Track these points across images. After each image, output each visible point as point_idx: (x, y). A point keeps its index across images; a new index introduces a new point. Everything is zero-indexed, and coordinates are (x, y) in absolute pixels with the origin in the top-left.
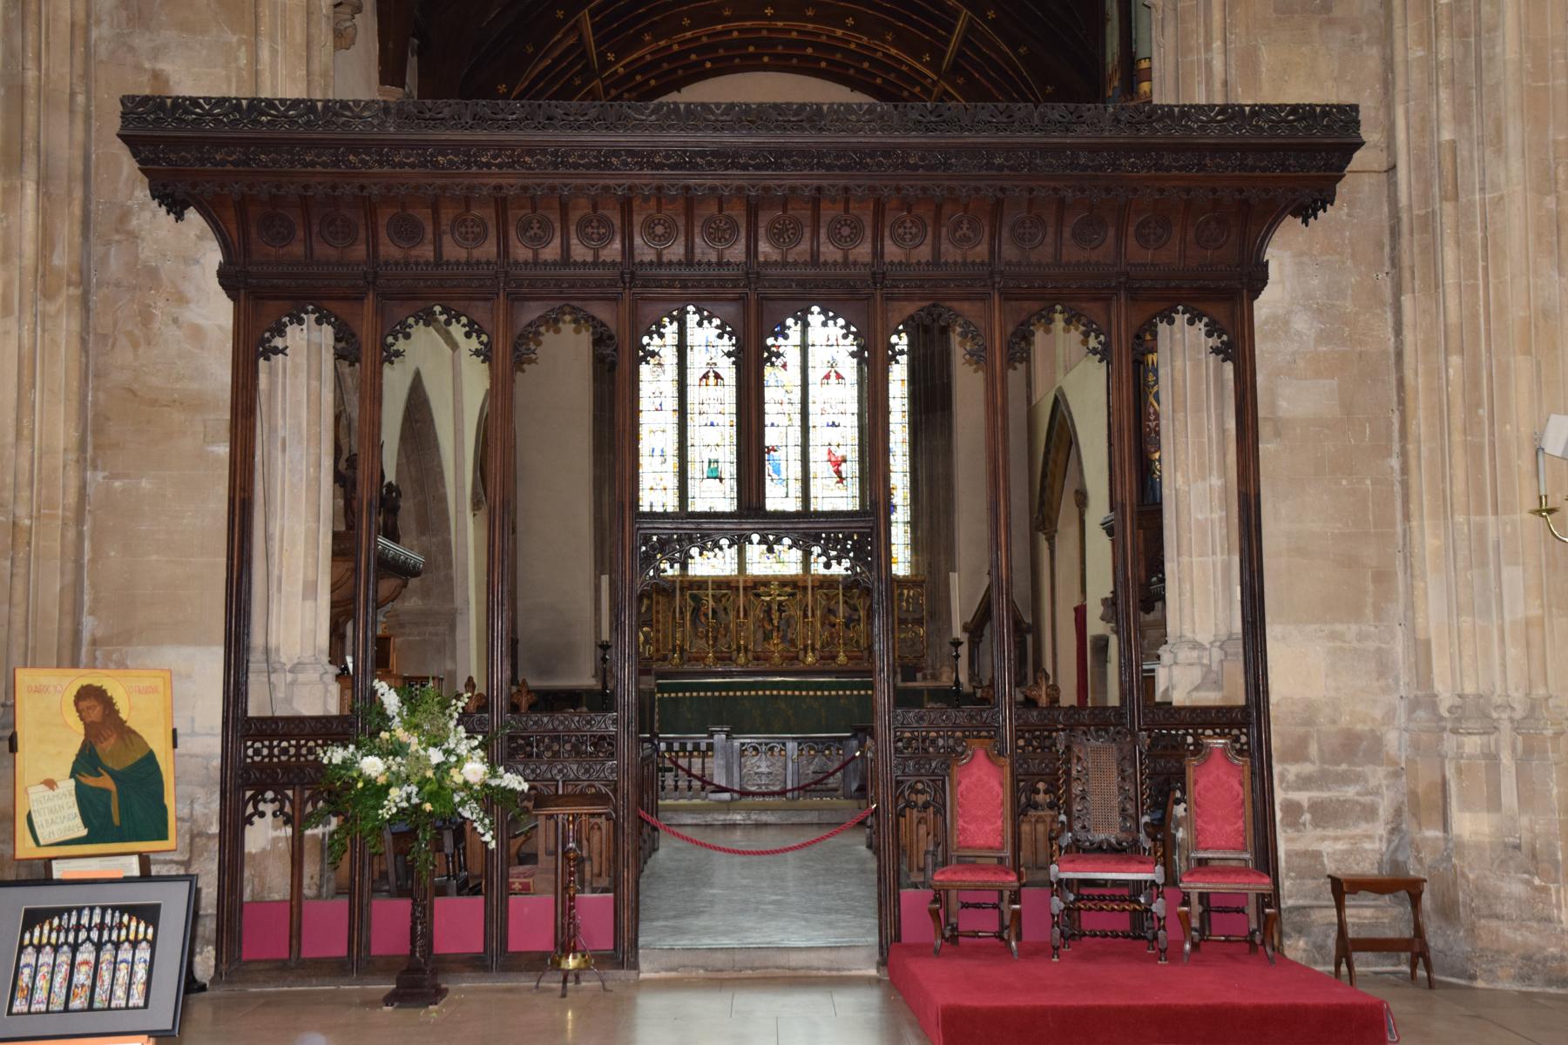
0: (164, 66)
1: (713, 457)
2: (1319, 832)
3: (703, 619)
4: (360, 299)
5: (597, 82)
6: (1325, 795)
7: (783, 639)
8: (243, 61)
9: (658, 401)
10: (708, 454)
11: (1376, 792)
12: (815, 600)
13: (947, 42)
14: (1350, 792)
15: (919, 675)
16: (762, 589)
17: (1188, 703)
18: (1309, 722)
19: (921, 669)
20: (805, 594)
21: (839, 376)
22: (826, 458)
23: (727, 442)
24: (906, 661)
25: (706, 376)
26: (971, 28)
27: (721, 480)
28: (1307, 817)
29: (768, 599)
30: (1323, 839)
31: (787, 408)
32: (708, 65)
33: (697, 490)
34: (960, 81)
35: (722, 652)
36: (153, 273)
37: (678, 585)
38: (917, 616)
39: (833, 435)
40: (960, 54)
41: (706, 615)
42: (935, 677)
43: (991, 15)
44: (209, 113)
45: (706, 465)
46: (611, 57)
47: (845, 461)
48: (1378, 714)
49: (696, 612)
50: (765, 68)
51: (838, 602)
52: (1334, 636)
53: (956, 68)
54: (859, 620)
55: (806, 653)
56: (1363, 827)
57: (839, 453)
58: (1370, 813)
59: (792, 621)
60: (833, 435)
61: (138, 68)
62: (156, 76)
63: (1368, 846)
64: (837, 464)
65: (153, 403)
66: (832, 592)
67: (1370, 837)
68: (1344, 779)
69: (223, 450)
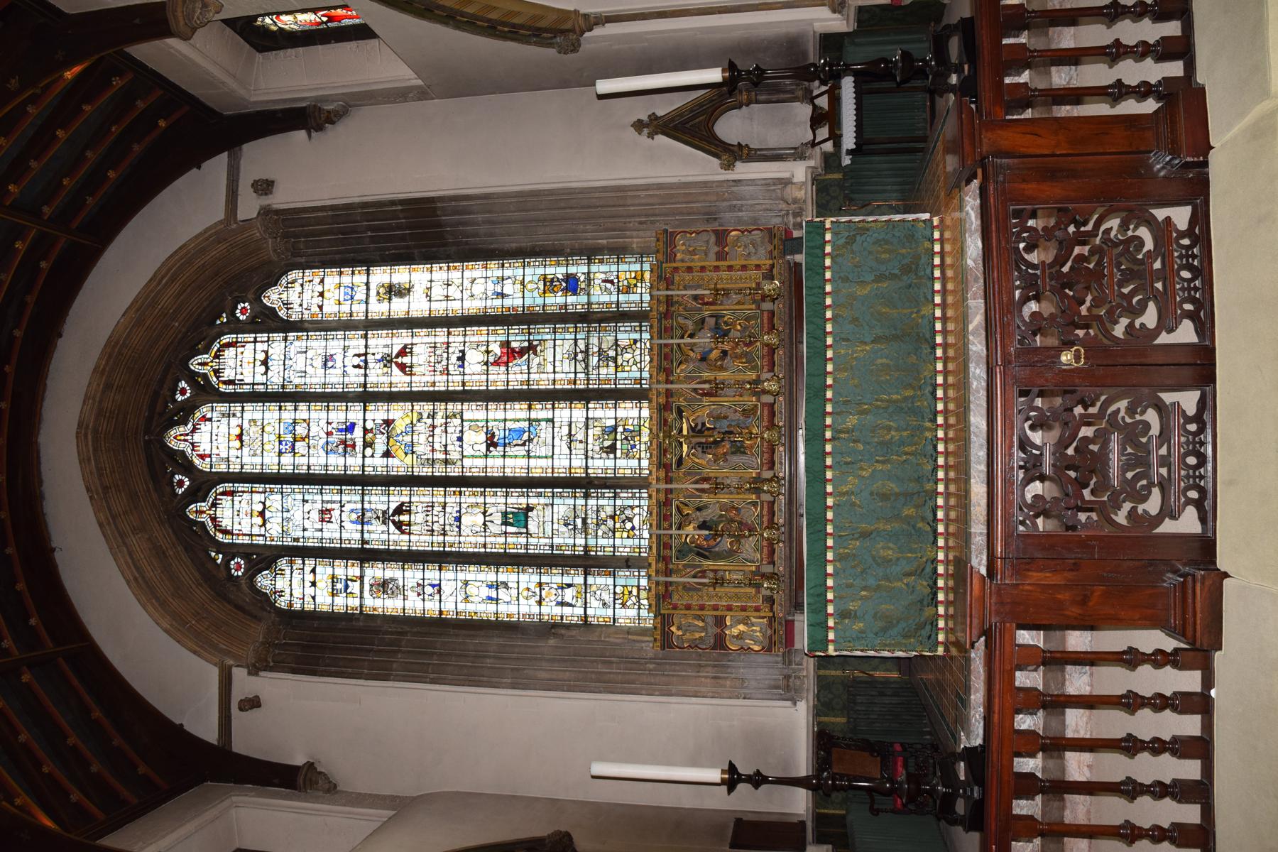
1: (498, 518)
9: (429, 590)
10: (496, 528)
12: (688, 379)
15: (796, 234)
19: (788, 232)
21: (402, 353)
22: (503, 369)
23: (481, 500)
24: (775, 253)
25: (399, 525)
27: (529, 509)
29: (685, 447)
31: (439, 420)
33: (543, 541)
35: (761, 515)
37: (662, 579)
38: (713, 239)
39: (475, 358)
45: (510, 529)
47: (508, 343)
49: (702, 553)
51: (692, 347)
54: (717, 317)
55: (765, 392)
57: (496, 349)
59: (715, 413)
60: (475, 358)
64: (510, 354)
66: (677, 356)
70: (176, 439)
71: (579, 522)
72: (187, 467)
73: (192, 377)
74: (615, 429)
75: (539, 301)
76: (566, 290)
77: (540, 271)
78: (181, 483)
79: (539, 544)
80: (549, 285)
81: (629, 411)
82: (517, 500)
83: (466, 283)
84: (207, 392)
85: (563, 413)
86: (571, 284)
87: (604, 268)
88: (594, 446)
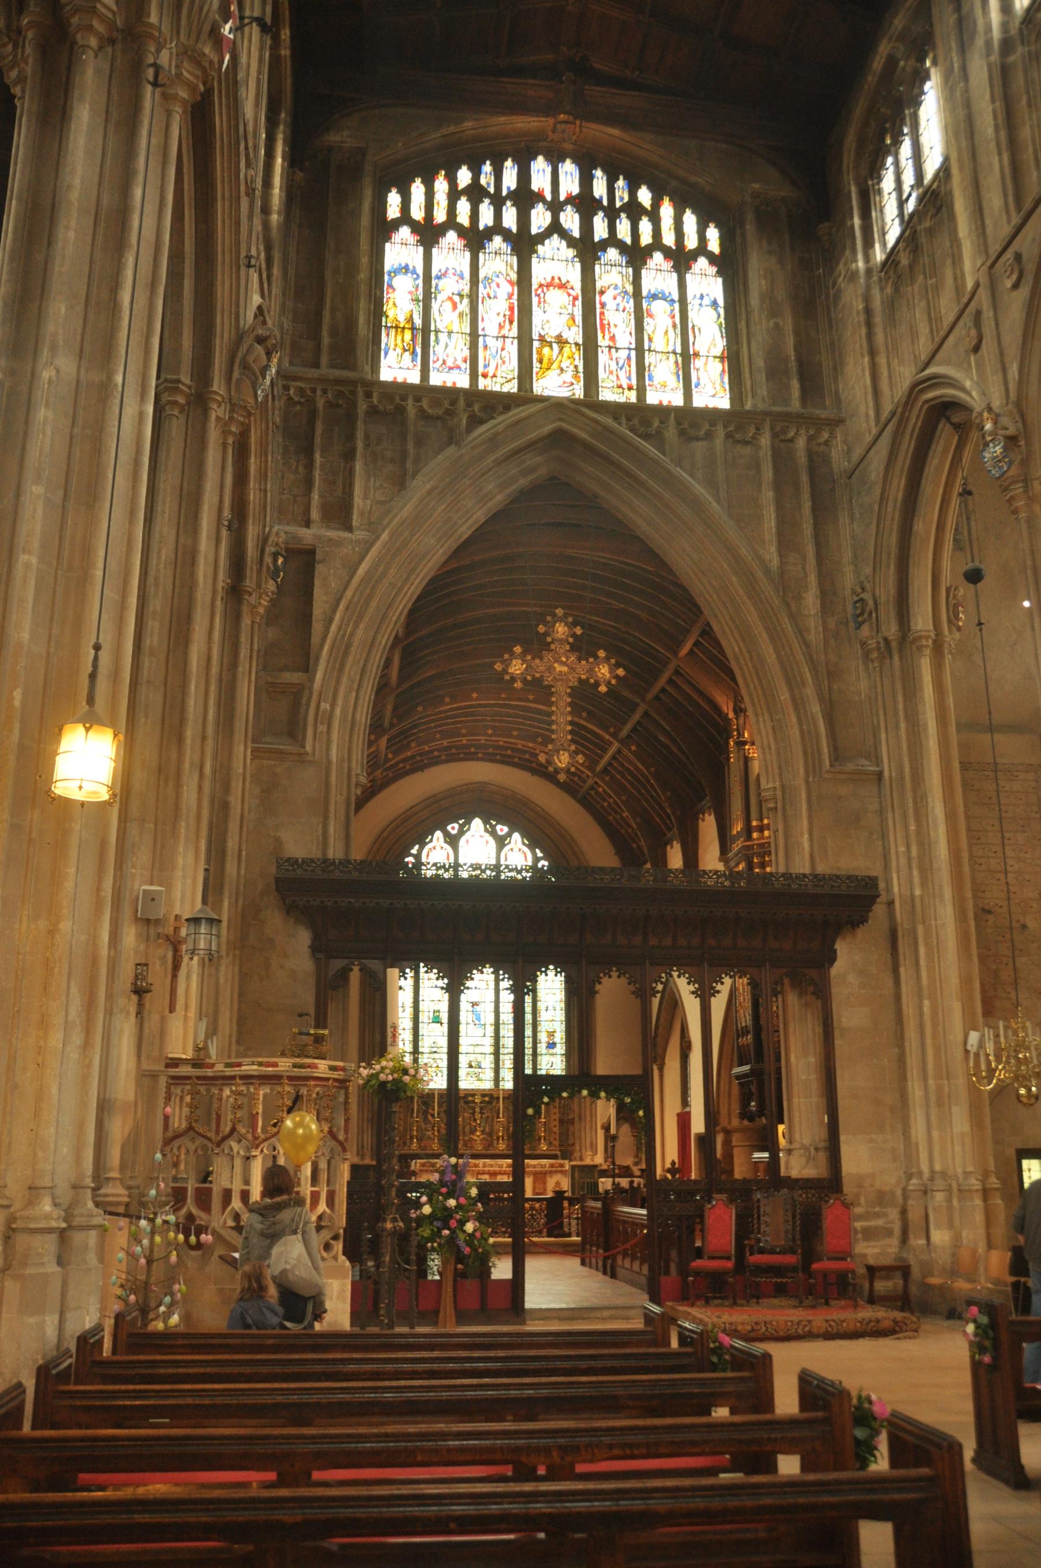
1: (437, 1008)
2: (865, 1244)
3: (430, 1117)
6: (869, 1224)
7: (483, 1132)
8: (320, 832)
10: (434, 1007)
11: (893, 1222)
13: (601, 757)
14: (880, 1222)
16: (470, 1098)
17: (799, 1176)
18: (860, 1186)
20: (498, 1102)
26: (619, 752)
27: (441, 1024)
28: (860, 1236)
30: (868, 1247)
32: (443, 757)
34: (607, 778)
40: (610, 764)
41: (433, 1116)
42: (581, 1159)
43: (633, 748)
44: (318, 866)
46: (390, 756)
48: (893, 1181)
50: (478, 759)
52: (871, 1141)
53: (605, 770)
56: (887, 1241)
58: (889, 1233)
62: (278, 841)
63: (890, 1250)
67: (891, 1246)
68: (877, 1215)
70: (477, 823)
71: (435, 1049)
72: (461, 832)
73: (509, 835)
74: (480, 1067)
75: (543, 1029)
76: (549, 1043)
77: (558, 1030)
78: (453, 828)
79: (423, 1029)
80: (551, 1034)
81: (489, 1074)
82: (445, 1017)
83: (553, 991)
84: (501, 842)
85: (489, 1041)
86: (551, 1045)
87: (559, 1062)
88: (472, 1057)
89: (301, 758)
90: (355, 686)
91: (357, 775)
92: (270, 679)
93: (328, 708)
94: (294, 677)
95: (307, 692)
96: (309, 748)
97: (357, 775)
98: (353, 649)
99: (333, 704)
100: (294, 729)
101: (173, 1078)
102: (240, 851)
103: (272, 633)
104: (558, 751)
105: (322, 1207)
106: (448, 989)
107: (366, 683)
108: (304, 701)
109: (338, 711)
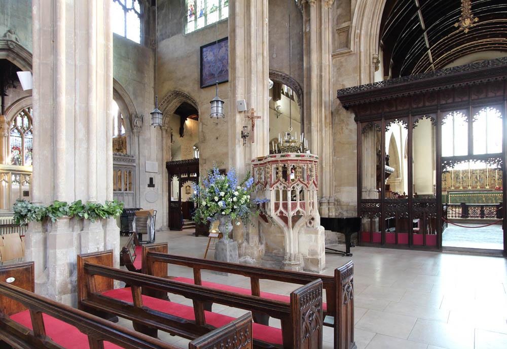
0: (344, 83)
4: (381, 120)
5: (432, 65)
8: (358, 78)
36: (343, 120)
61: (340, 84)
62: (343, 85)
65: (343, 144)
69: (356, 151)
89: (350, 53)
90: (371, 21)
91: (373, 55)
92: (337, 28)
93: (359, 32)
94: (345, 25)
95: (351, 28)
96: (352, 49)
97: (373, 55)
98: (367, 5)
99: (361, 31)
100: (347, 44)
101: (255, 165)
102: (329, 91)
103: (339, 11)
104: (464, 20)
105: (298, 208)
106: (407, 127)
107: (375, 19)
108: (350, 32)
109: (363, 32)
